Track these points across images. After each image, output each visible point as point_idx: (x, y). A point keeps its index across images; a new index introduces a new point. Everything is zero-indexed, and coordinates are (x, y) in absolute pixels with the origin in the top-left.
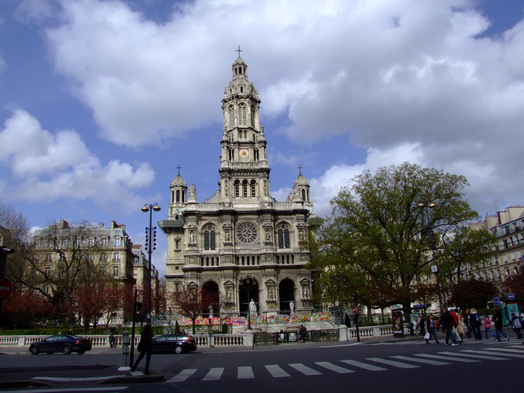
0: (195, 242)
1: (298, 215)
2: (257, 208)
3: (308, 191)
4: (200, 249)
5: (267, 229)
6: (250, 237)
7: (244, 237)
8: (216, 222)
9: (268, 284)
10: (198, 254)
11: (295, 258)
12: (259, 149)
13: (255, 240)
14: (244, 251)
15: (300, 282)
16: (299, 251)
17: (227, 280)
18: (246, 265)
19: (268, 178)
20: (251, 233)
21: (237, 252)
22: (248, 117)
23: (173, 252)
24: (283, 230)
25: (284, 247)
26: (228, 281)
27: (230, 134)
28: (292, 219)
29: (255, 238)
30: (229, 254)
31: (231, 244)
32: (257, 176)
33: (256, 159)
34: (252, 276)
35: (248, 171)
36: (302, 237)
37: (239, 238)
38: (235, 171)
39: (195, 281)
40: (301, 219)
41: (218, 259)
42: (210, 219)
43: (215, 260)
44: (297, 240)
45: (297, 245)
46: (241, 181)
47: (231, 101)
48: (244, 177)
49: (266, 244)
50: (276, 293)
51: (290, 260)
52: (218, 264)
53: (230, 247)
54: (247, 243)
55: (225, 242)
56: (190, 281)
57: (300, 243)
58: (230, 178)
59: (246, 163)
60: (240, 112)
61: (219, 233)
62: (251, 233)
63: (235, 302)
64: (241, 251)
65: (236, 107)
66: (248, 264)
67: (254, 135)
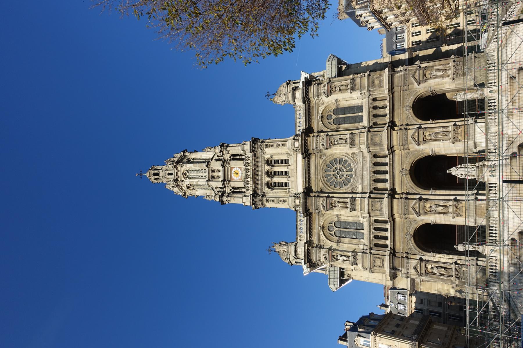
1: (311, 94)
3: (294, 83)
4: (362, 247)
5: (330, 144)
6: (343, 168)
7: (343, 178)
8: (321, 218)
9: (421, 140)
10: (368, 251)
12: (231, 153)
13: (349, 160)
15: (419, 84)
17: (411, 210)
20: (338, 166)
21: (366, 191)
22: (197, 167)
24: (334, 117)
25: (360, 114)
28: (318, 105)
29: (346, 161)
32: (261, 156)
33: (243, 157)
34: (407, 166)
35: (255, 169)
36: (344, 87)
39: (413, 263)
40: (318, 91)
41: (376, 221)
42: (316, 229)
45: (356, 94)
46: (268, 179)
48: (263, 174)
49: (353, 144)
50: (438, 125)
52: (385, 222)
53: (358, 202)
54: (352, 173)
55: (349, 209)
56: (413, 271)
57: (353, 89)
58: (263, 196)
60: (193, 177)
61: (337, 215)
62: (338, 166)
65: (187, 182)
66: (385, 172)
67: (216, 160)
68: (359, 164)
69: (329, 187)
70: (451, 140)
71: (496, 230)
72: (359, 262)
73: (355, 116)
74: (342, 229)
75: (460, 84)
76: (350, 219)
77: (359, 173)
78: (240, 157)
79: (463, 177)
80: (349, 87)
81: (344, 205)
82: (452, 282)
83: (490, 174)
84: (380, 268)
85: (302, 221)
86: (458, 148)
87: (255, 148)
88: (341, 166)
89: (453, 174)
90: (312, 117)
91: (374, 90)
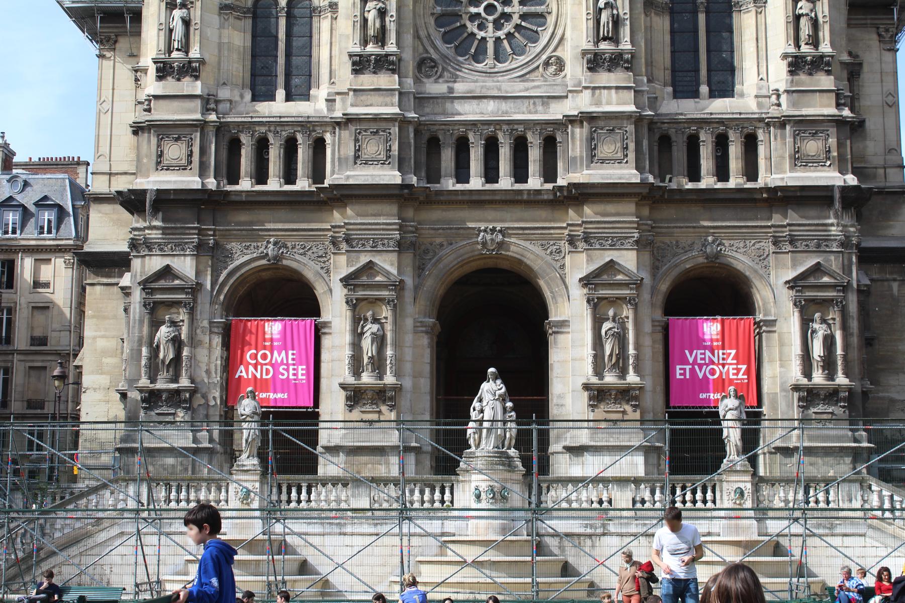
0: (195, 53)
4: (224, 93)
6: (508, 27)
7: (472, 27)
11: (762, 150)
15: (792, 284)
16: (786, 108)
17: (364, 259)
18: (476, 183)
23: (125, 138)
25: (704, 89)
26: (370, 265)
29: (534, 37)
30: (376, 119)
37: (447, 38)
39: (186, 266)
41: (319, 146)
43: (303, 154)
44: (779, 43)
49: (595, 62)
51: (735, 163)
52: (318, 174)
54: (490, 61)
55: (357, 49)
56: (155, 263)
57: (796, 64)
63: (407, 383)
66: (491, 174)
68: (520, 86)
70: (594, 380)
71: (309, 501)
72: (171, 86)
73: (697, 70)
74: (282, 22)
75: (774, 408)
76: (322, 53)
77: (490, 84)
79: (474, 415)
80: (805, 49)
81: (371, 32)
82: (131, 382)
83: (483, 486)
84: (154, 158)
86: (568, 401)
88: (516, 19)
89: (485, 387)
91: (783, 138)
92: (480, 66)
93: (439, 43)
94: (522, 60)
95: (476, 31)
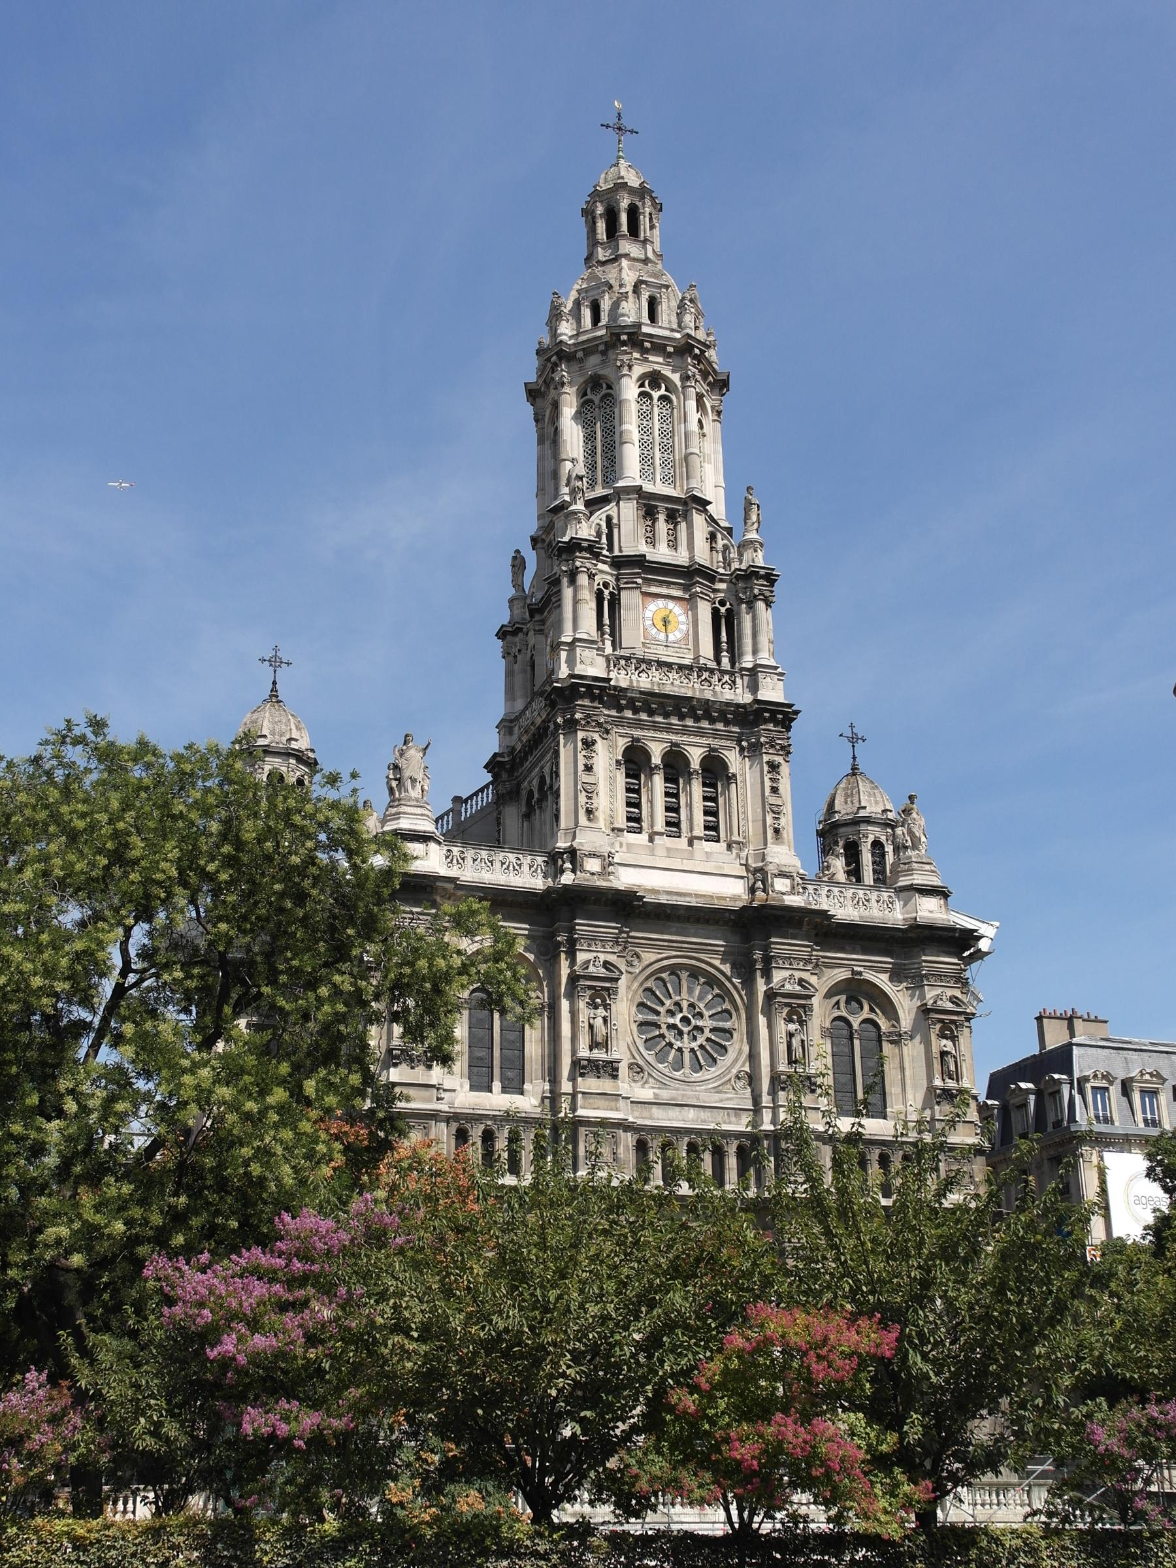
2: (735, 898)
6: (701, 1040)
13: (724, 1061)
14: (674, 1112)
19: (786, 751)
27: (599, 517)
31: (610, 1069)
38: (632, 698)
47: (594, 360)
54: (687, 1070)
55: (584, 1053)
59: (681, 667)
62: (707, 1023)
64: (655, 1110)
69: (641, 984)
78: (725, 646)
85: (525, 875)
87: (766, 721)
88: (707, 1034)
90: (858, 948)
92: (678, 1075)
93: (642, 1049)
94: (714, 1071)
95: (673, 1041)
